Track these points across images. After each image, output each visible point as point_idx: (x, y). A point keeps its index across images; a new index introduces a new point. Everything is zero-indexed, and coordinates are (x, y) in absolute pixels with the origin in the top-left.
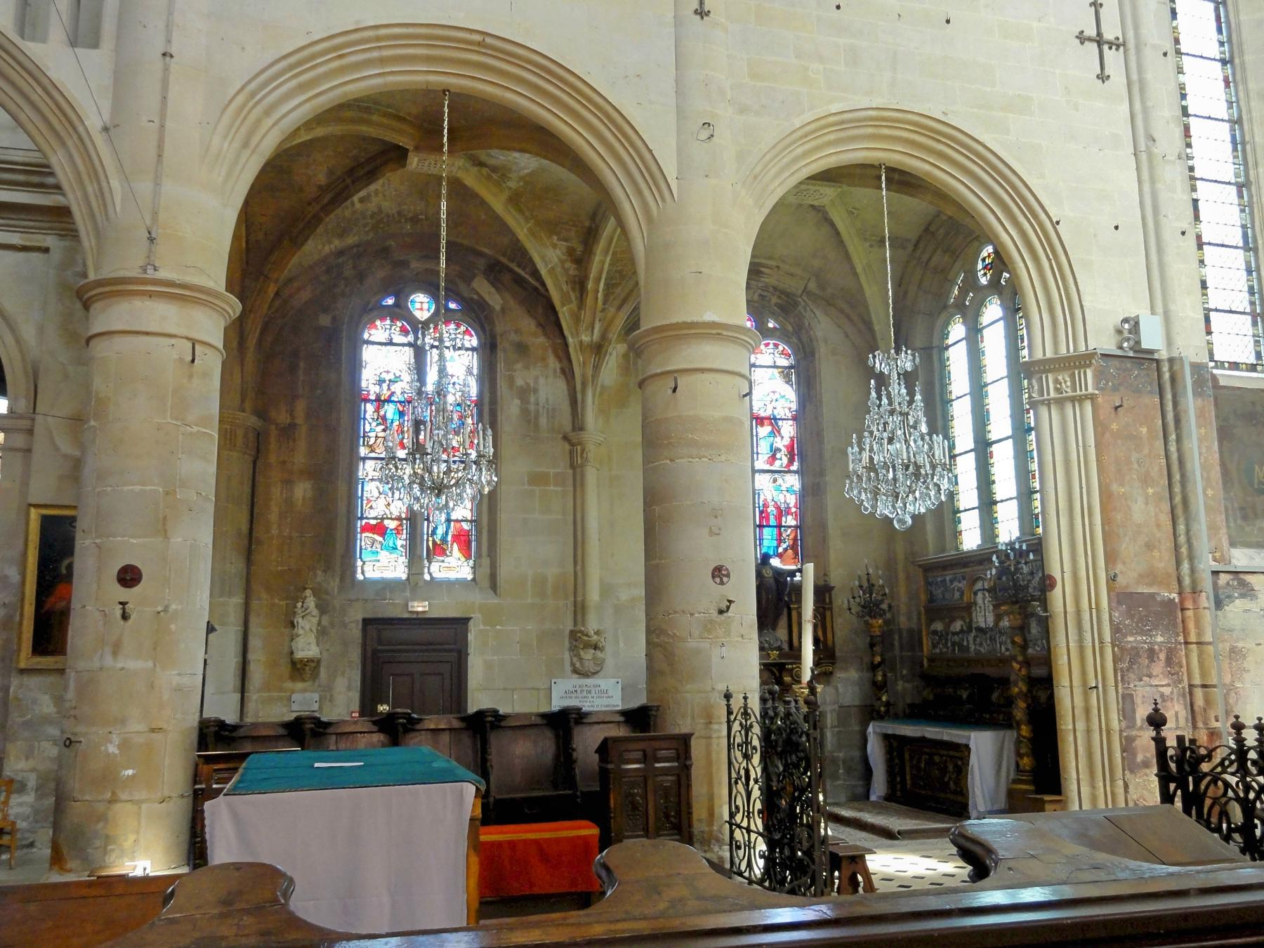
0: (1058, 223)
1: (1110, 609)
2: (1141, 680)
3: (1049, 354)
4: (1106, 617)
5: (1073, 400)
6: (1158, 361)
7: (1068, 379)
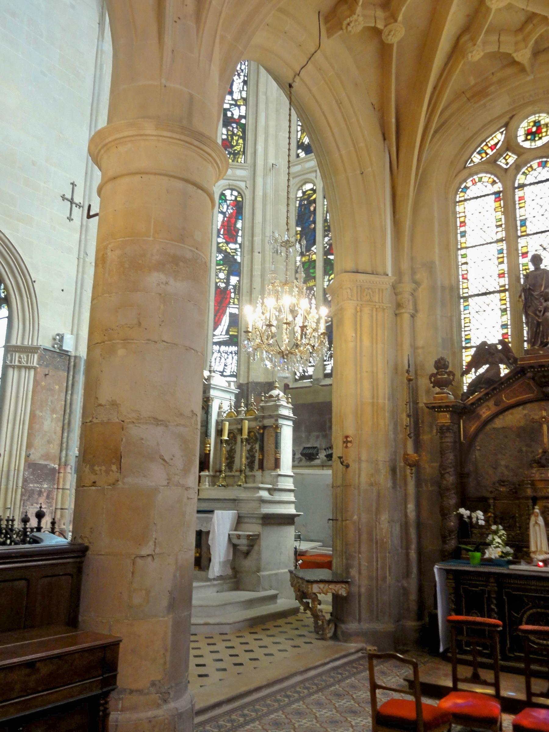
0: (34, 282)
1: (24, 470)
2: (32, 505)
3: (19, 343)
4: (21, 474)
5: (26, 367)
6: (70, 356)
7: (25, 357)
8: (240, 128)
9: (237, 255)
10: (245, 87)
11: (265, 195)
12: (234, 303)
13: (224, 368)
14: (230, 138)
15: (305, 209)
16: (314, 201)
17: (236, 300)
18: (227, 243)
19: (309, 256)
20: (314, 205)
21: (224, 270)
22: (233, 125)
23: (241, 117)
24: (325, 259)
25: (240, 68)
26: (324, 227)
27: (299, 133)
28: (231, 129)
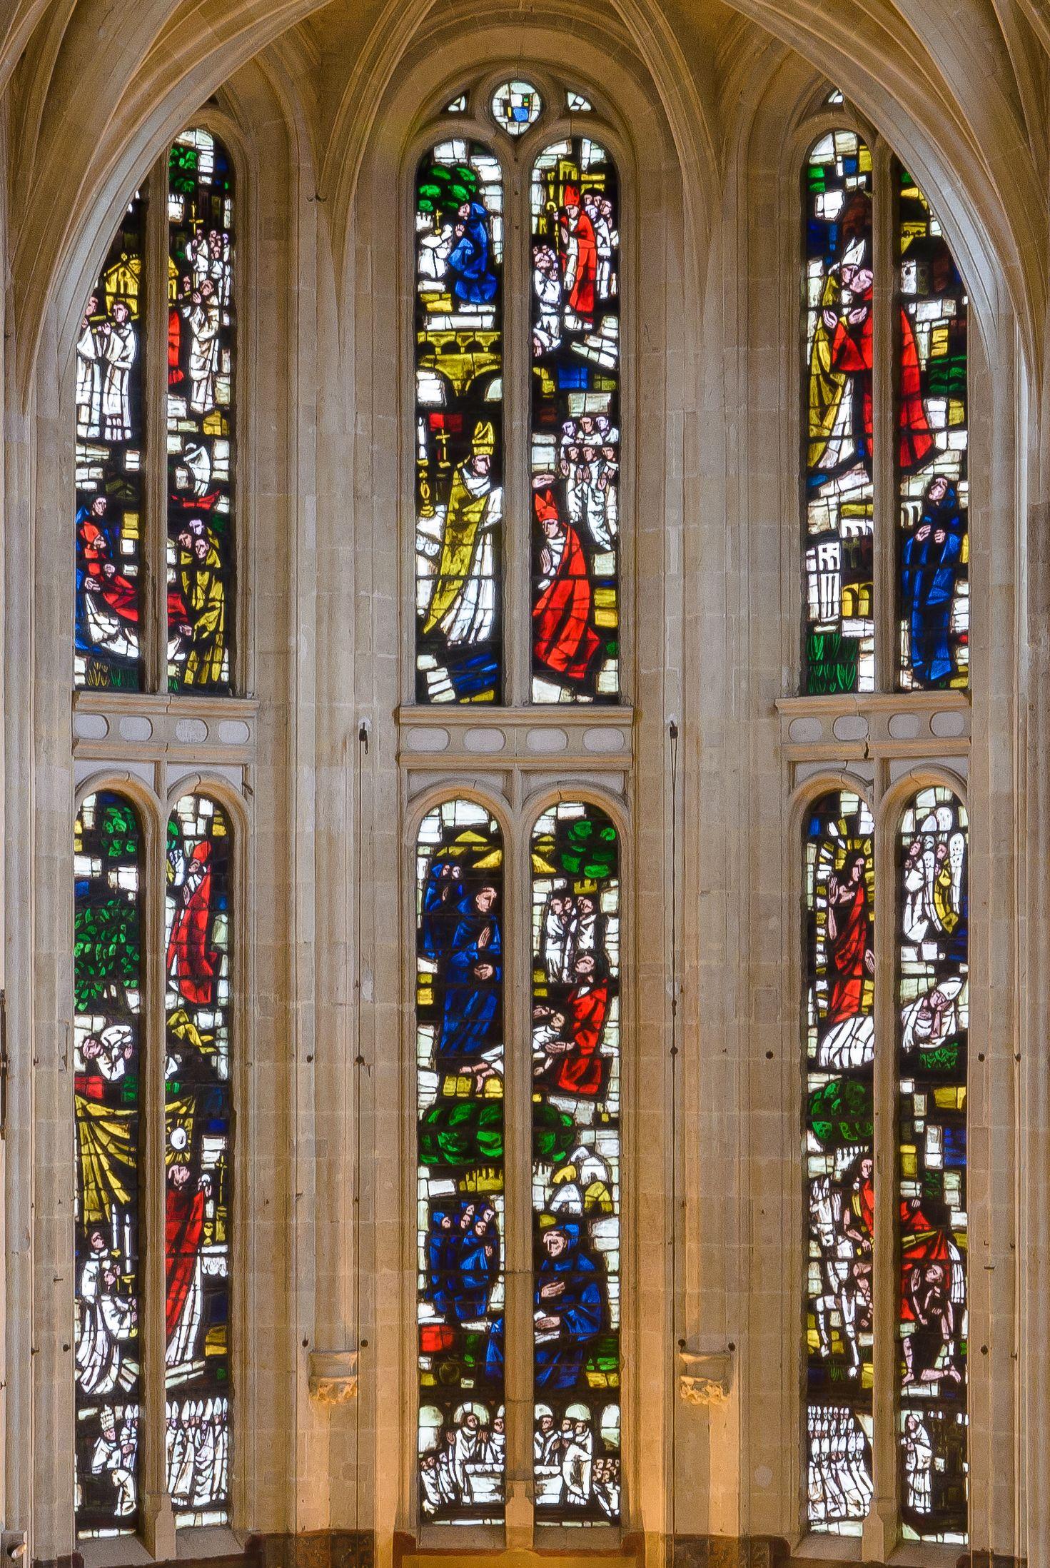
8: (216, 535)
9: (218, 1053)
10: (226, 357)
11: (326, 840)
12: (213, 1236)
13: (194, 1483)
14: (185, 583)
15: (455, 897)
16: (496, 877)
17: (219, 1225)
18: (190, 1010)
19: (472, 1077)
20: (492, 893)
21: (186, 1116)
22: (193, 523)
23: (217, 488)
24: (535, 1105)
25: (209, 273)
26: (535, 986)
27: (425, 588)
28: (188, 542)
